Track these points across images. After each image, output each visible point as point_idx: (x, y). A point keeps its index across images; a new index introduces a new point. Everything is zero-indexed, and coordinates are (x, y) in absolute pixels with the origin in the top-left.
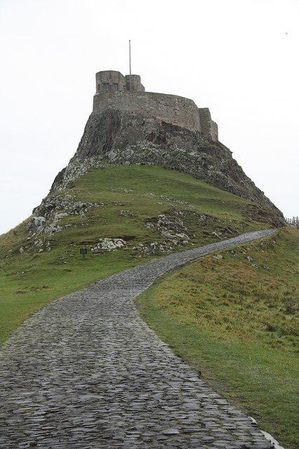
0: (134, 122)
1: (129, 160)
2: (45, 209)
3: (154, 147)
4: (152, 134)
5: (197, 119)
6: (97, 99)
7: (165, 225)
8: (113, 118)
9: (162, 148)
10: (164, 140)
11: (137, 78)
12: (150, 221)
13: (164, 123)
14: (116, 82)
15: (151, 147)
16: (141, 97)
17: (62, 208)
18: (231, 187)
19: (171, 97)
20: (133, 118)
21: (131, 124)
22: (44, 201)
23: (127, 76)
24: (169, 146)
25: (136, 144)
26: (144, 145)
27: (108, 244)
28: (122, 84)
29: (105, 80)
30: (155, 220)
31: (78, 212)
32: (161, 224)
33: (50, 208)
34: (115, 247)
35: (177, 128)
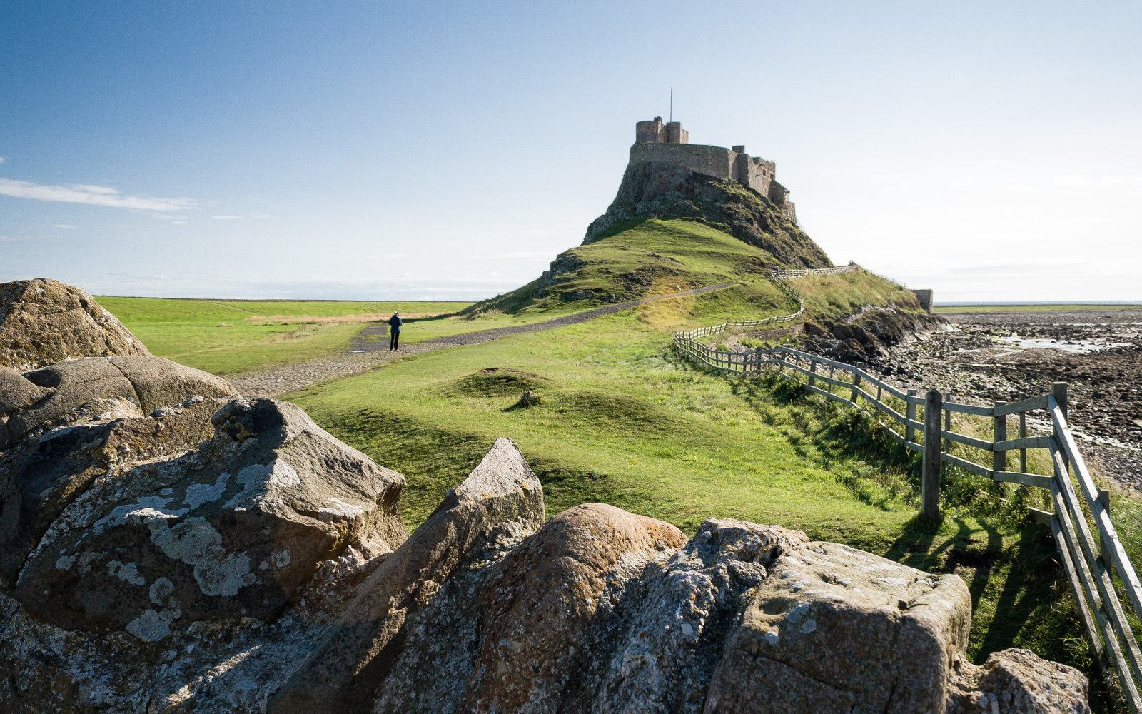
0: (664, 174)
4: (681, 186)
6: (634, 150)
10: (692, 191)
11: (677, 125)
13: (694, 173)
20: (664, 169)
21: (661, 176)
23: (668, 124)
29: (644, 130)
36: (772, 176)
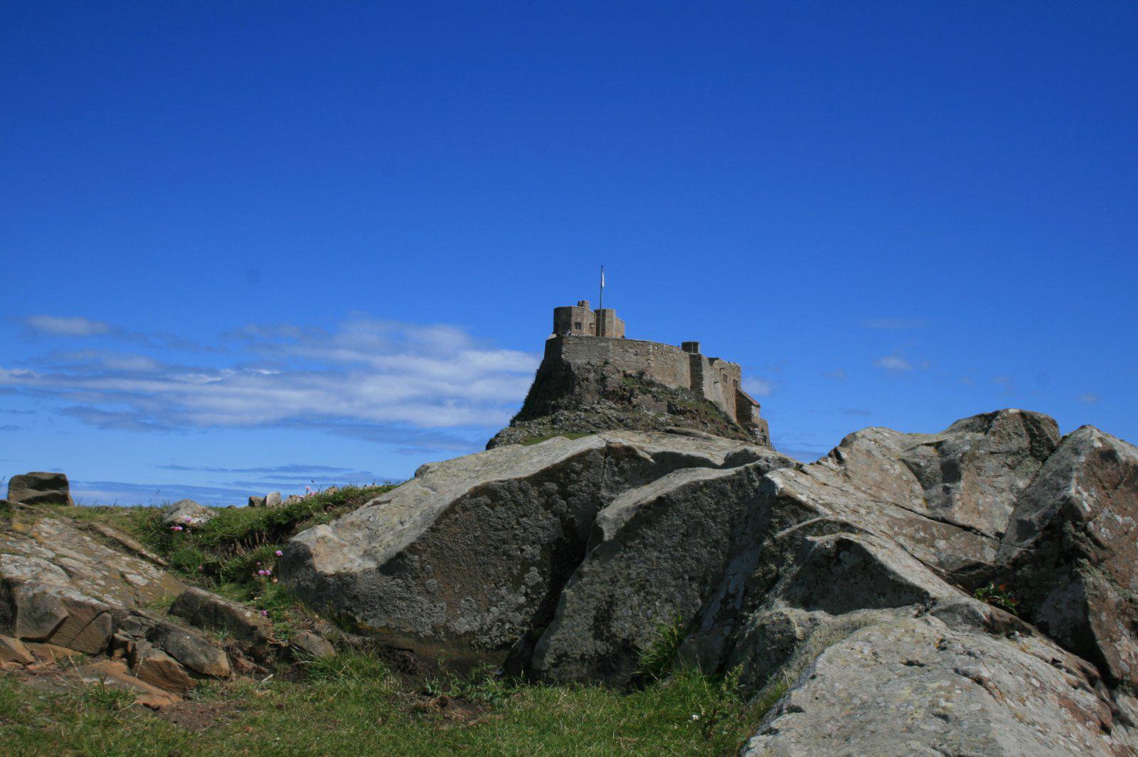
3: (614, 408)
5: (685, 368)
6: (550, 344)
9: (625, 410)
14: (579, 320)
15: (611, 408)
16: (603, 344)
20: (589, 371)
21: (587, 379)
23: (597, 312)
28: (588, 319)
36: (736, 383)
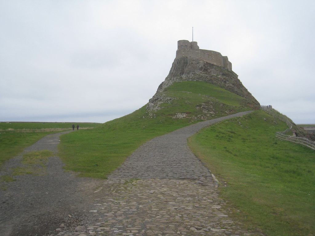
0: (194, 62)
1: (191, 79)
2: (153, 100)
3: (202, 73)
6: (178, 52)
7: (205, 108)
8: (184, 60)
9: (206, 74)
11: (196, 43)
12: (198, 106)
13: (207, 62)
14: (187, 45)
15: (201, 73)
16: (197, 51)
17: (161, 100)
18: (236, 92)
19: (210, 51)
21: (192, 63)
22: (154, 97)
24: (209, 73)
25: (194, 72)
26: (198, 72)
27: (180, 116)
30: (200, 106)
31: (168, 101)
32: (203, 108)
33: (156, 100)
34: (182, 117)
35: (213, 65)
